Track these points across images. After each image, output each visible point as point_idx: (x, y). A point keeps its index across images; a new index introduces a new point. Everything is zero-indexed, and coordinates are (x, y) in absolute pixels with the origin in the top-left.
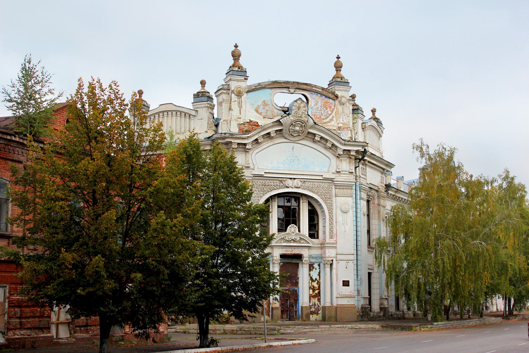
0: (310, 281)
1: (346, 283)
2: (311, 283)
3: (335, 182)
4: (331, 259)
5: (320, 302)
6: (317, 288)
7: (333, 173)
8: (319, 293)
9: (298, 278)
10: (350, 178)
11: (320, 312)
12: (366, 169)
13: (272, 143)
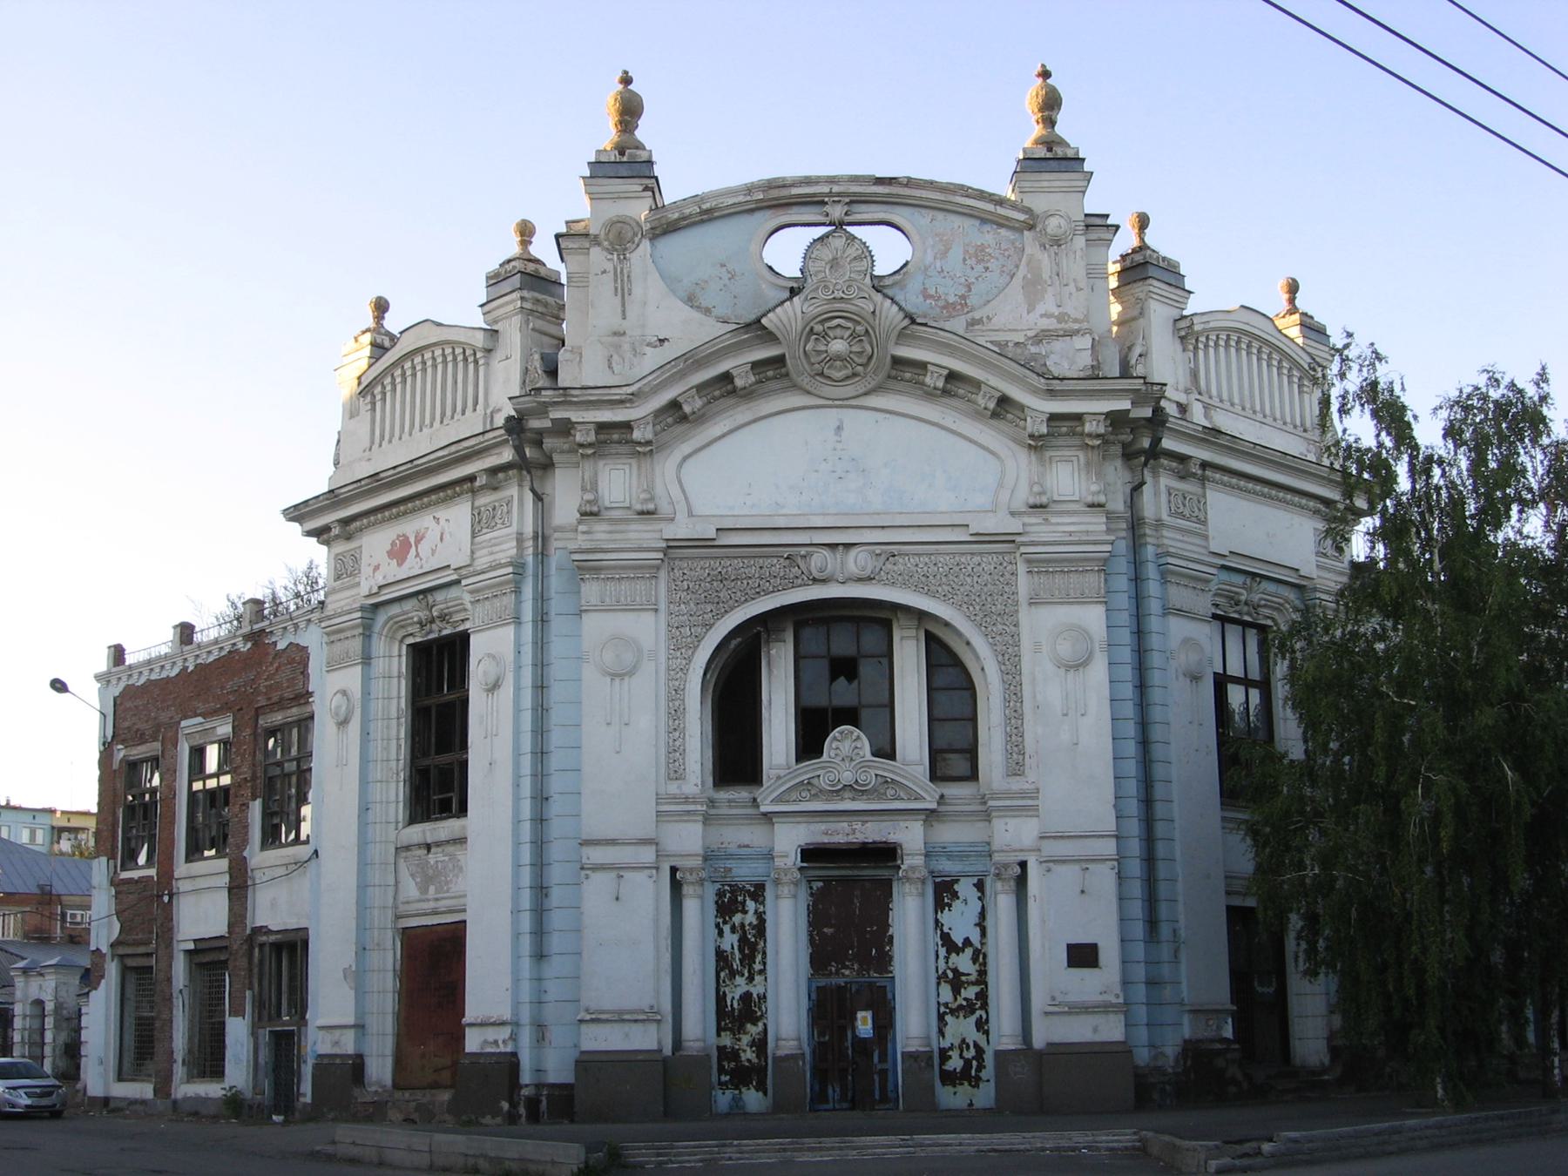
0: (943, 952)
1: (1083, 956)
2: (947, 958)
3: (1023, 549)
4: (1021, 857)
5: (987, 1033)
6: (973, 978)
7: (1013, 514)
8: (983, 996)
9: (891, 937)
10: (1091, 528)
11: (988, 1072)
12: (1201, 500)
13: (748, 416)
